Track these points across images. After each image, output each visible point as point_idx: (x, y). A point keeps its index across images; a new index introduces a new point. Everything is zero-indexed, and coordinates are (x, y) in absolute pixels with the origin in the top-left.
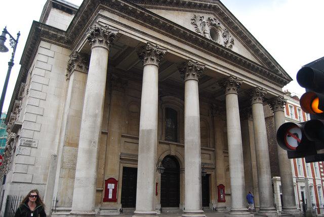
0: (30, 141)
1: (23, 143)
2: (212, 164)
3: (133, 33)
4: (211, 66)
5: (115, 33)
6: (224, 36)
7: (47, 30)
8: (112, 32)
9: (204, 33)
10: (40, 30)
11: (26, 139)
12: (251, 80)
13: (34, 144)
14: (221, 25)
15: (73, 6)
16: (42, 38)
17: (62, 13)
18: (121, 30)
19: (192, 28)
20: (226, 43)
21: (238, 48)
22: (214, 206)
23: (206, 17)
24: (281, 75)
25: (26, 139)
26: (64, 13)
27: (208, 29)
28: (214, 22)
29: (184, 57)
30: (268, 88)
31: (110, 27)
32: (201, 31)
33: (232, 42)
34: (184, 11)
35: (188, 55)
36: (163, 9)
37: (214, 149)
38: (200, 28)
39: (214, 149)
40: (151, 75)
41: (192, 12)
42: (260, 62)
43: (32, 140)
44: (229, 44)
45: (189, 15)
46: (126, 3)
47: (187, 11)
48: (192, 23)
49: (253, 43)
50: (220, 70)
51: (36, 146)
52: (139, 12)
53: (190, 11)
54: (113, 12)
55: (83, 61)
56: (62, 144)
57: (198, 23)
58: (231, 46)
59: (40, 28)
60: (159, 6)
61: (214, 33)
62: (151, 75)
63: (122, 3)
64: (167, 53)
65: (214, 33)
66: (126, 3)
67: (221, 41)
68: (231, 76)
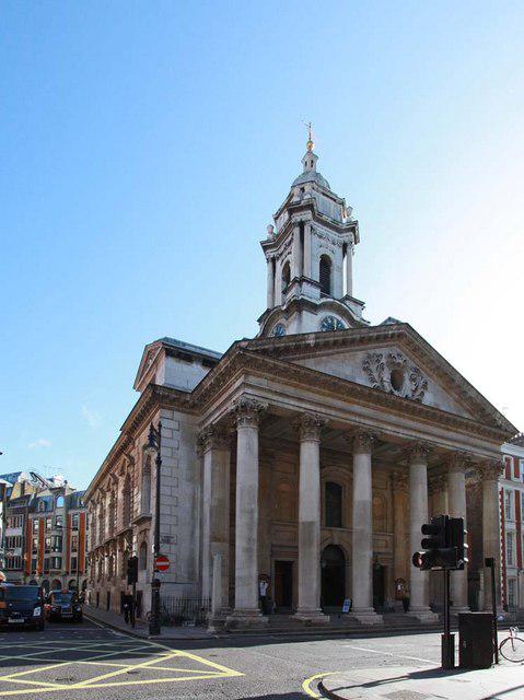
2: (389, 553)
5: (265, 405)
6: (413, 380)
12: (448, 440)
15: (193, 349)
22: (391, 606)
23: (384, 351)
24: (499, 427)
27: (386, 376)
30: (479, 449)
33: (425, 386)
38: (375, 375)
40: (310, 453)
48: (364, 369)
50: (403, 434)
55: (224, 437)
56: (206, 540)
57: (373, 367)
58: (422, 393)
61: (396, 382)
62: (310, 453)
65: (396, 382)
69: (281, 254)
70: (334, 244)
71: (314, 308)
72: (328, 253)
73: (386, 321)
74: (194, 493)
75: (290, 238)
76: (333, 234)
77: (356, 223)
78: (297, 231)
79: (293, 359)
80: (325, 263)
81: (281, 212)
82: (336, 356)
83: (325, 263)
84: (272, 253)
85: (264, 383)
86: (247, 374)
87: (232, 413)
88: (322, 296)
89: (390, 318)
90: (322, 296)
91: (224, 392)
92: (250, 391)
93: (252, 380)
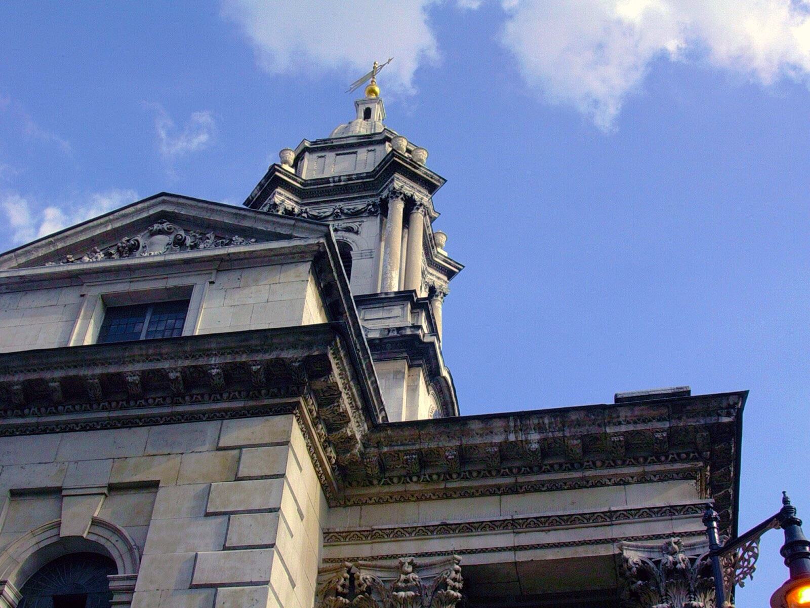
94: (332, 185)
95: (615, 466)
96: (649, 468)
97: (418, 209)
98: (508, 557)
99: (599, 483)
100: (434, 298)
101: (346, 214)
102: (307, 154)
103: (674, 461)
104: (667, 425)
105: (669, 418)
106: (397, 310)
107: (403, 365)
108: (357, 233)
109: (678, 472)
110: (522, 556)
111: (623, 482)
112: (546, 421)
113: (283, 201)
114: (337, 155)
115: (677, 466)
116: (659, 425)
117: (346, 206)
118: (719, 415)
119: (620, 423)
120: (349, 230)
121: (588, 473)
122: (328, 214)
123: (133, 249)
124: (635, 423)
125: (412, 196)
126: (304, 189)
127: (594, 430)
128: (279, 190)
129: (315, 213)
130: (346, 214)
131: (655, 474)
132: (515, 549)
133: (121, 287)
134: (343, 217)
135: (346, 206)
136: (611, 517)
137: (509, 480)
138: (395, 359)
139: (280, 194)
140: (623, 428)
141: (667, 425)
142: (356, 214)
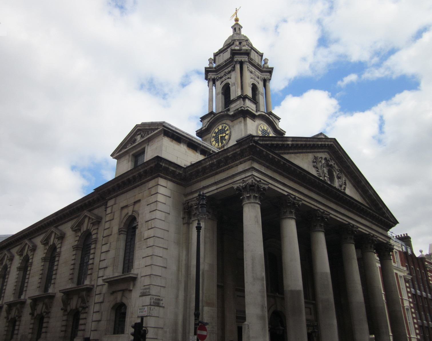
0: (159, 300)
1: (152, 302)
3: (276, 184)
4: (333, 215)
5: (266, 187)
6: (339, 178)
7: (167, 166)
8: (264, 186)
9: (325, 176)
10: (161, 166)
11: (155, 297)
13: (161, 302)
14: (336, 166)
15: (186, 135)
16: (160, 174)
17: (172, 141)
18: (271, 184)
19: (313, 172)
20: (341, 186)
21: (350, 191)
24: (387, 218)
25: (155, 297)
26: (174, 142)
27: (326, 170)
28: (330, 163)
29: (313, 207)
31: (262, 181)
32: (321, 174)
33: (345, 184)
34: (306, 152)
35: (315, 204)
36: (293, 153)
37: (314, 302)
39: (314, 302)
41: (313, 152)
42: (367, 203)
43: (159, 298)
44: (343, 188)
45: (310, 157)
46: (274, 155)
47: (308, 152)
48: (314, 166)
49: (363, 183)
50: (340, 218)
51: (163, 305)
52: (282, 163)
53: (310, 152)
54: (260, 163)
58: (345, 189)
59: (161, 164)
60: (291, 151)
63: (271, 155)
64: (303, 204)
66: (274, 155)
67: (337, 184)
68: (349, 223)
69: (221, 78)
70: (258, 78)
71: (253, 117)
72: (256, 83)
73: (318, 135)
74: (179, 255)
75: (229, 69)
76: (258, 73)
77: (272, 69)
78: (238, 67)
79: (283, 153)
80: (254, 88)
81: (221, 51)
82: (298, 155)
83: (254, 88)
84: (211, 76)
85: (263, 169)
86: (253, 160)
87: (238, 189)
88: (257, 112)
89: (321, 134)
90: (257, 112)
91: (224, 171)
92: (256, 174)
93: (256, 166)
94: (222, 65)
95: (234, 162)
96: (241, 160)
97: (244, 63)
98: (216, 192)
99: (232, 167)
100: (266, 82)
101: (227, 73)
102: (216, 57)
103: (245, 157)
104: (239, 149)
105: (239, 148)
106: (238, 102)
107: (241, 119)
108: (230, 78)
109: (247, 159)
110: (219, 190)
111: (237, 165)
112: (216, 156)
113: (211, 77)
114: (223, 53)
115: (246, 158)
116: (237, 150)
117: (227, 70)
118: (250, 143)
119: (230, 152)
120: (228, 78)
121: (230, 165)
122: (223, 75)
123: (135, 141)
124: (233, 151)
125: (241, 60)
126: (216, 70)
127: (226, 155)
128: (209, 74)
129: (220, 76)
130: (227, 73)
131: (243, 161)
132: (217, 189)
133: (134, 152)
134: (227, 74)
135: (227, 70)
136: (233, 176)
137: (214, 172)
138: (239, 118)
139: (210, 75)
140: (231, 153)
141: (239, 149)
142: (229, 72)
